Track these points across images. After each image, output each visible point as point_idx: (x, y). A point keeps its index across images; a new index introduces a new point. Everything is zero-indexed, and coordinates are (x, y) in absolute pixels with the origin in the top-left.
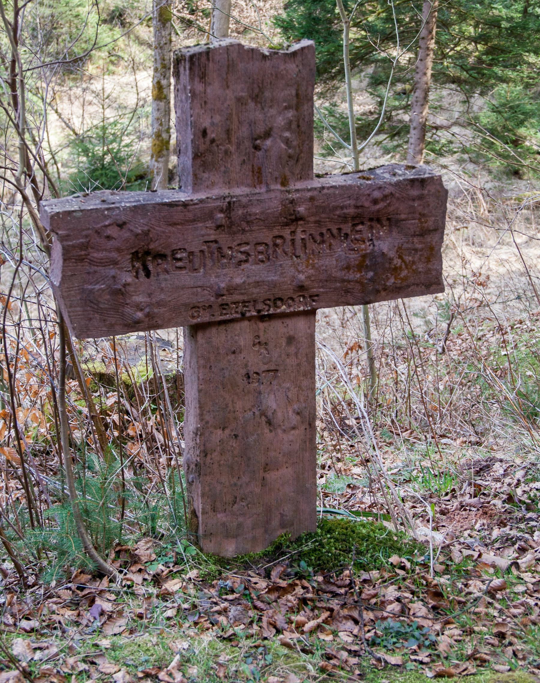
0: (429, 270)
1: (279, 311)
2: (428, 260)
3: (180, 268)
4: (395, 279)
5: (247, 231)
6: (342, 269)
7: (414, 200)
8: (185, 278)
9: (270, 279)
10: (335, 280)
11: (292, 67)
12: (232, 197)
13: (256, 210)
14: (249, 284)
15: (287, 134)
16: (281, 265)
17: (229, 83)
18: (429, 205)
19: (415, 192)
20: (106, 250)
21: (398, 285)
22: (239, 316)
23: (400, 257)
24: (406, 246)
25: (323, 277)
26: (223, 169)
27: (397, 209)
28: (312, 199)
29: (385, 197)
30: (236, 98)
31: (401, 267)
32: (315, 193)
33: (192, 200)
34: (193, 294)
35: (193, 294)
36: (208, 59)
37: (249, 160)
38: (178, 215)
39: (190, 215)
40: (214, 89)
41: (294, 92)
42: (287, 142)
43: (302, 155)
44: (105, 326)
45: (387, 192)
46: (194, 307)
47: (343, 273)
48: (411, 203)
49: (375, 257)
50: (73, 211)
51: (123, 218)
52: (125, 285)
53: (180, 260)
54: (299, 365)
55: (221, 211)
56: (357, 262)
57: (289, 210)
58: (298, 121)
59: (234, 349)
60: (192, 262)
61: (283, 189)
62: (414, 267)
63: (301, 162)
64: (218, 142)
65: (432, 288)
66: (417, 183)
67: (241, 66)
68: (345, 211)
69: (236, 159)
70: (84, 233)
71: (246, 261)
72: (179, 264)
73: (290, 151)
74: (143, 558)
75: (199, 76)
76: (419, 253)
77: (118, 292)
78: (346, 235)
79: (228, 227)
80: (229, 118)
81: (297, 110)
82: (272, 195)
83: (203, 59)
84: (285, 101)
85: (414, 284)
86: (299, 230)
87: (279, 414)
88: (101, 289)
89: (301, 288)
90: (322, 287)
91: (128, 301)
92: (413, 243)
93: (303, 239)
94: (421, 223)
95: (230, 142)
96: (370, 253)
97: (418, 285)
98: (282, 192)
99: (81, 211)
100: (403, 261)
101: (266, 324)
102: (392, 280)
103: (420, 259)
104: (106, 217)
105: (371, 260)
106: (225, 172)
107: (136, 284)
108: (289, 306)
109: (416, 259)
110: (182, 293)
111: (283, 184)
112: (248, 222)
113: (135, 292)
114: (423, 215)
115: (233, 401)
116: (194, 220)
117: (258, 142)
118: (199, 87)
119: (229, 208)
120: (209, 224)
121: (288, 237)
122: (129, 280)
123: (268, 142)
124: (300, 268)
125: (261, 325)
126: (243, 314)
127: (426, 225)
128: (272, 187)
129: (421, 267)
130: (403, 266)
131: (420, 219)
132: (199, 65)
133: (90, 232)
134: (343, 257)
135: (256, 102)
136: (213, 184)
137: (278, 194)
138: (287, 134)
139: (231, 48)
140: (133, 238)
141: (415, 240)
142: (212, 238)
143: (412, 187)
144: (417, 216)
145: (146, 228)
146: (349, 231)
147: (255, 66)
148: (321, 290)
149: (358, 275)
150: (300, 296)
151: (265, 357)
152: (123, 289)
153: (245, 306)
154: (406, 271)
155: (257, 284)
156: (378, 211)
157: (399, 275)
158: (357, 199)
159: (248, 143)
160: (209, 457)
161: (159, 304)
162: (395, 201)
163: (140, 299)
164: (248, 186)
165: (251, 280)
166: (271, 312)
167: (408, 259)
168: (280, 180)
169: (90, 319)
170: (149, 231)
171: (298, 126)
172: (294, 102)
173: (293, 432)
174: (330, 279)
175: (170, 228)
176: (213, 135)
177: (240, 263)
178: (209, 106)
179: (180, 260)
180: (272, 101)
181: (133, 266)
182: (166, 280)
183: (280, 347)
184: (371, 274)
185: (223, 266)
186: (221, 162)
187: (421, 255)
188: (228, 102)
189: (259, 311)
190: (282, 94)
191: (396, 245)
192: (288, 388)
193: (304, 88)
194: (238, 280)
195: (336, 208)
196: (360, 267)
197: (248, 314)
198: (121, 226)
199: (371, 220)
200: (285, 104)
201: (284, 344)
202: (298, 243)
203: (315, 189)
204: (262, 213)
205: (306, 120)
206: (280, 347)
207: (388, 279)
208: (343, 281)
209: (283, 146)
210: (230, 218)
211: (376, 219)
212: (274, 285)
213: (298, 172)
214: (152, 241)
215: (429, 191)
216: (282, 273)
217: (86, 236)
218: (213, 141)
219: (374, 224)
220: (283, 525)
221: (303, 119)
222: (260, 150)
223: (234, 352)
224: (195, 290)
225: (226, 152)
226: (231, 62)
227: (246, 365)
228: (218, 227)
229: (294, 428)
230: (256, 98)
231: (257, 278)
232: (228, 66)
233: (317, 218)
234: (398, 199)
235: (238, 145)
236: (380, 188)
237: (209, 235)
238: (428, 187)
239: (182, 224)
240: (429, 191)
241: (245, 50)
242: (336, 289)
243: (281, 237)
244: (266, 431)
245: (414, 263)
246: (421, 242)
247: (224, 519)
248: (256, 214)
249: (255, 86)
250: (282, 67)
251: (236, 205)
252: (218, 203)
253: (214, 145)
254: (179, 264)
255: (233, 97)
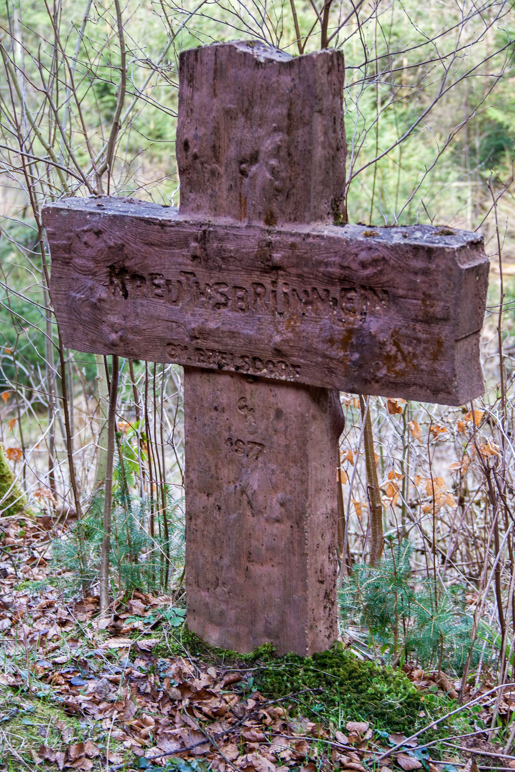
0: (435, 370)
1: (258, 373)
2: (435, 358)
3: (160, 296)
4: (389, 370)
5: (224, 270)
6: (324, 342)
7: (416, 273)
8: (161, 308)
9: (245, 331)
10: (316, 352)
11: (286, 80)
12: (209, 226)
13: (230, 246)
14: (223, 332)
15: (273, 162)
16: (259, 319)
17: (217, 92)
18: (437, 285)
19: (418, 264)
20: (84, 257)
21: (392, 380)
22: (215, 367)
23: (396, 344)
24: (404, 331)
25: (303, 344)
26: (209, 191)
27: (393, 279)
28: (293, 246)
29: (375, 262)
30: (224, 109)
31: (395, 357)
32: (298, 240)
33: (170, 221)
34: (168, 328)
35: (168, 328)
36: (196, 59)
37: (236, 186)
38: (155, 236)
39: (166, 238)
40: (201, 96)
41: (285, 112)
42: (273, 171)
43: (294, 191)
44: (88, 340)
45: (376, 255)
46: (169, 344)
47: (326, 346)
48: (412, 277)
49: (362, 336)
50: (62, 209)
51: (100, 226)
52: (100, 300)
53: (158, 286)
54: (287, 446)
55: (196, 239)
56: (341, 337)
57: (265, 254)
58: (288, 148)
59: (215, 405)
60: (169, 291)
61: (267, 227)
62: (415, 361)
63: (292, 199)
64: (202, 159)
65: (441, 396)
66: (421, 253)
67: (232, 72)
68: (330, 269)
69: (225, 183)
70: (68, 234)
71: (225, 305)
72: (159, 291)
73: (277, 183)
74: (134, 609)
75: (188, 79)
76: (423, 345)
77: (94, 306)
78: (335, 300)
79: (204, 260)
80: (216, 131)
81: (289, 133)
82: (251, 232)
83: (192, 58)
84: (274, 121)
85: (415, 384)
86: (281, 281)
87: (261, 498)
88: (80, 299)
89: (278, 352)
90: (302, 357)
91: (104, 319)
92: (414, 329)
93: (285, 293)
94: (426, 306)
95: (218, 161)
96: (358, 330)
97: (421, 387)
98: (263, 230)
99: (68, 210)
100: (399, 349)
101: (253, 387)
102: (384, 371)
103: (424, 354)
104: (87, 222)
105: (358, 338)
106: (211, 196)
107: (111, 302)
108: (271, 372)
109: (418, 352)
110: (156, 324)
111: (268, 222)
112: (223, 259)
113: (111, 310)
114: (427, 296)
115: (216, 466)
116: (171, 245)
117: (244, 166)
118: (188, 92)
119: (204, 238)
120: (185, 252)
121: (269, 287)
122: (104, 295)
123: (254, 169)
124: (280, 328)
125: (248, 387)
126: (220, 366)
127: (432, 310)
128: (255, 223)
129: (424, 364)
130: (400, 357)
131: (423, 300)
132: (188, 65)
133: (72, 234)
134: (328, 327)
135: (246, 117)
136: (199, 208)
137: (258, 233)
138: (273, 162)
139: (221, 49)
140: (107, 249)
141: (418, 326)
142: (189, 269)
143: (415, 256)
144: (420, 295)
145: (119, 242)
146: (337, 296)
147: (245, 74)
148: (302, 361)
149: (341, 354)
150: (282, 362)
151: (250, 425)
152: (98, 304)
153: (223, 358)
154: (403, 365)
155: (233, 334)
156: (368, 278)
157: (393, 366)
158: (343, 257)
159: (234, 166)
160: (193, 522)
161: (135, 330)
162: (389, 269)
163: (113, 318)
164: (234, 217)
165: (225, 328)
166: (249, 372)
167: (407, 349)
168: (264, 217)
169: (75, 329)
170: (123, 246)
171: (289, 155)
172: (285, 123)
173: (277, 525)
174: (309, 350)
175: (146, 247)
176: (195, 150)
177: (218, 305)
178: (195, 115)
179: (158, 286)
180: (261, 118)
181: (112, 282)
182: (142, 305)
183: (268, 419)
184: (356, 356)
185: (203, 305)
186: (208, 183)
187: (425, 348)
188: (214, 114)
189: (237, 368)
190: (272, 112)
191: (392, 327)
192: (273, 471)
193: (299, 108)
194: (212, 325)
195: (320, 263)
196: (345, 343)
197: (226, 368)
198: (98, 233)
199: (363, 287)
200: (274, 125)
201: (272, 417)
202: (280, 297)
203: (300, 234)
204: (237, 251)
205: (300, 148)
206: (268, 419)
207: (379, 369)
208: (325, 356)
209: (268, 176)
210: (205, 250)
211: (371, 288)
212: (250, 341)
213: (289, 210)
214: (127, 257)
215: (438, 266)
216: (259, 329)
217: (69, 238)
218: (195, 157)
219: (370, 295)
220: (268, 634)
221: (296, 147)
222: (247, 176)
223: (216, 409)
224: (170, 324)
225: (213, 173)
226: (219, 66)
227: (230, 429)
228: (194, 257)
229: (278, 521)
230: (247, 113)
231: (232, 327)
232: (215, 71)
233: (300, 272)
234: (394, 268)
235: (227, 166)
236: (370, 249)
237: (186, 265)
238: (437, 260)
239: (159, 246)
240: (438, 266)
241: (237, 54)
242: (317, 364)
243: (262, 285)
244: (249, 513)
245: (415, 356)
246: (425, 331)
247: (207, 599)
248: (231, 251)
249: (245, 98)
250: (274, 79)
251: (212, 235)
252: (194, 230)
253: (197, 161)
254: (159, 291)
255: (220, 108)
